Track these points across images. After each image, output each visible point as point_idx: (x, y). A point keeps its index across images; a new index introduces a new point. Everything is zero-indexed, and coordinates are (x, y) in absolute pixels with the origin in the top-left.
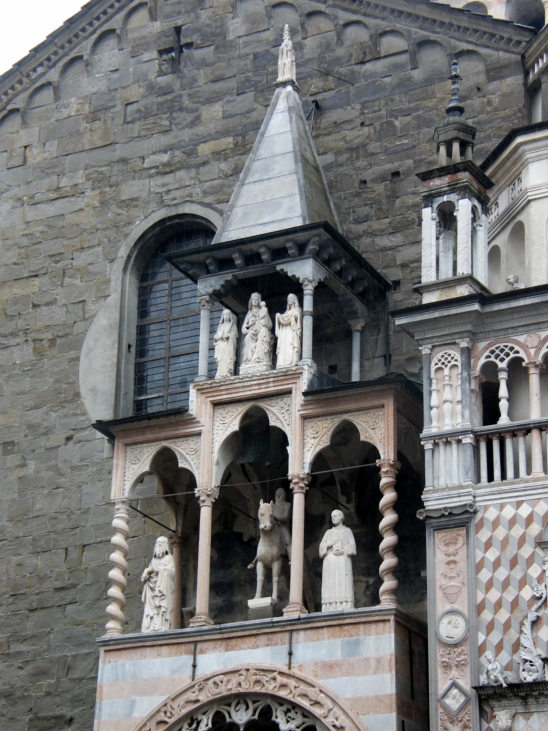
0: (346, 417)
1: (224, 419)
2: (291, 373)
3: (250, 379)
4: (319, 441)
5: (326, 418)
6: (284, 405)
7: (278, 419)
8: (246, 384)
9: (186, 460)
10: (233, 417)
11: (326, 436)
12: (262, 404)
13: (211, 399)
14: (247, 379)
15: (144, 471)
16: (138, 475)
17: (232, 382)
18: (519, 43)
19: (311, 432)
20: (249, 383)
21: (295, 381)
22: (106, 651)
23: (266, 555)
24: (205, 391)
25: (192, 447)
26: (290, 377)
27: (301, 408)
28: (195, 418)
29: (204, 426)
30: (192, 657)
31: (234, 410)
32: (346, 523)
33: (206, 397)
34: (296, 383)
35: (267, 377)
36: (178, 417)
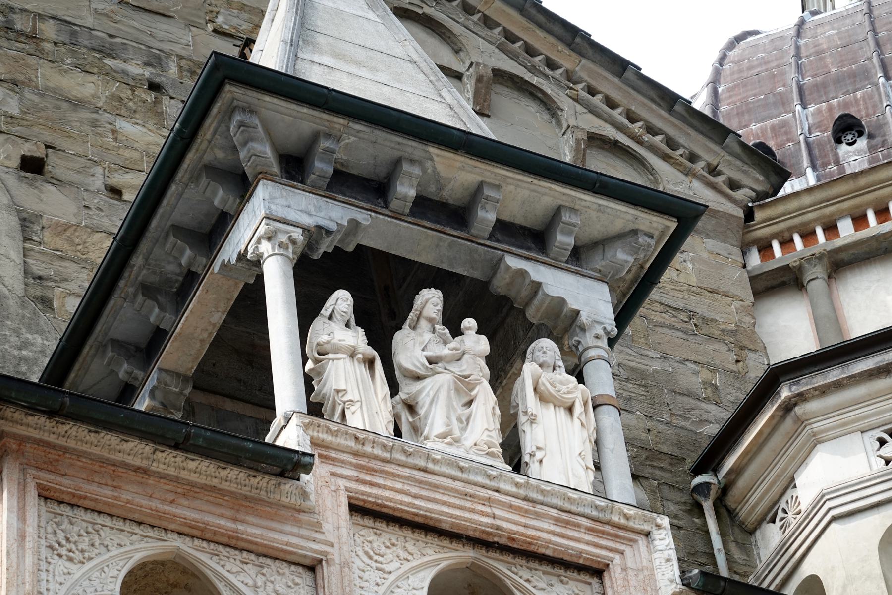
1: (380, 559)
2: (616, 518)
3: (487, 482)
10: (407, 566)
13: (353, 485)
14: (480, 479)
17: (430, 466)
18: (734, 185)
20: (483, 493)
24: (333, 454)
26: (607, 528)
28: (311, 511)
29: (332, 546)
31: (410, 546)
33: (333, 474)
34: (622, 553)
35: (540, 497)
36: (264, 482)
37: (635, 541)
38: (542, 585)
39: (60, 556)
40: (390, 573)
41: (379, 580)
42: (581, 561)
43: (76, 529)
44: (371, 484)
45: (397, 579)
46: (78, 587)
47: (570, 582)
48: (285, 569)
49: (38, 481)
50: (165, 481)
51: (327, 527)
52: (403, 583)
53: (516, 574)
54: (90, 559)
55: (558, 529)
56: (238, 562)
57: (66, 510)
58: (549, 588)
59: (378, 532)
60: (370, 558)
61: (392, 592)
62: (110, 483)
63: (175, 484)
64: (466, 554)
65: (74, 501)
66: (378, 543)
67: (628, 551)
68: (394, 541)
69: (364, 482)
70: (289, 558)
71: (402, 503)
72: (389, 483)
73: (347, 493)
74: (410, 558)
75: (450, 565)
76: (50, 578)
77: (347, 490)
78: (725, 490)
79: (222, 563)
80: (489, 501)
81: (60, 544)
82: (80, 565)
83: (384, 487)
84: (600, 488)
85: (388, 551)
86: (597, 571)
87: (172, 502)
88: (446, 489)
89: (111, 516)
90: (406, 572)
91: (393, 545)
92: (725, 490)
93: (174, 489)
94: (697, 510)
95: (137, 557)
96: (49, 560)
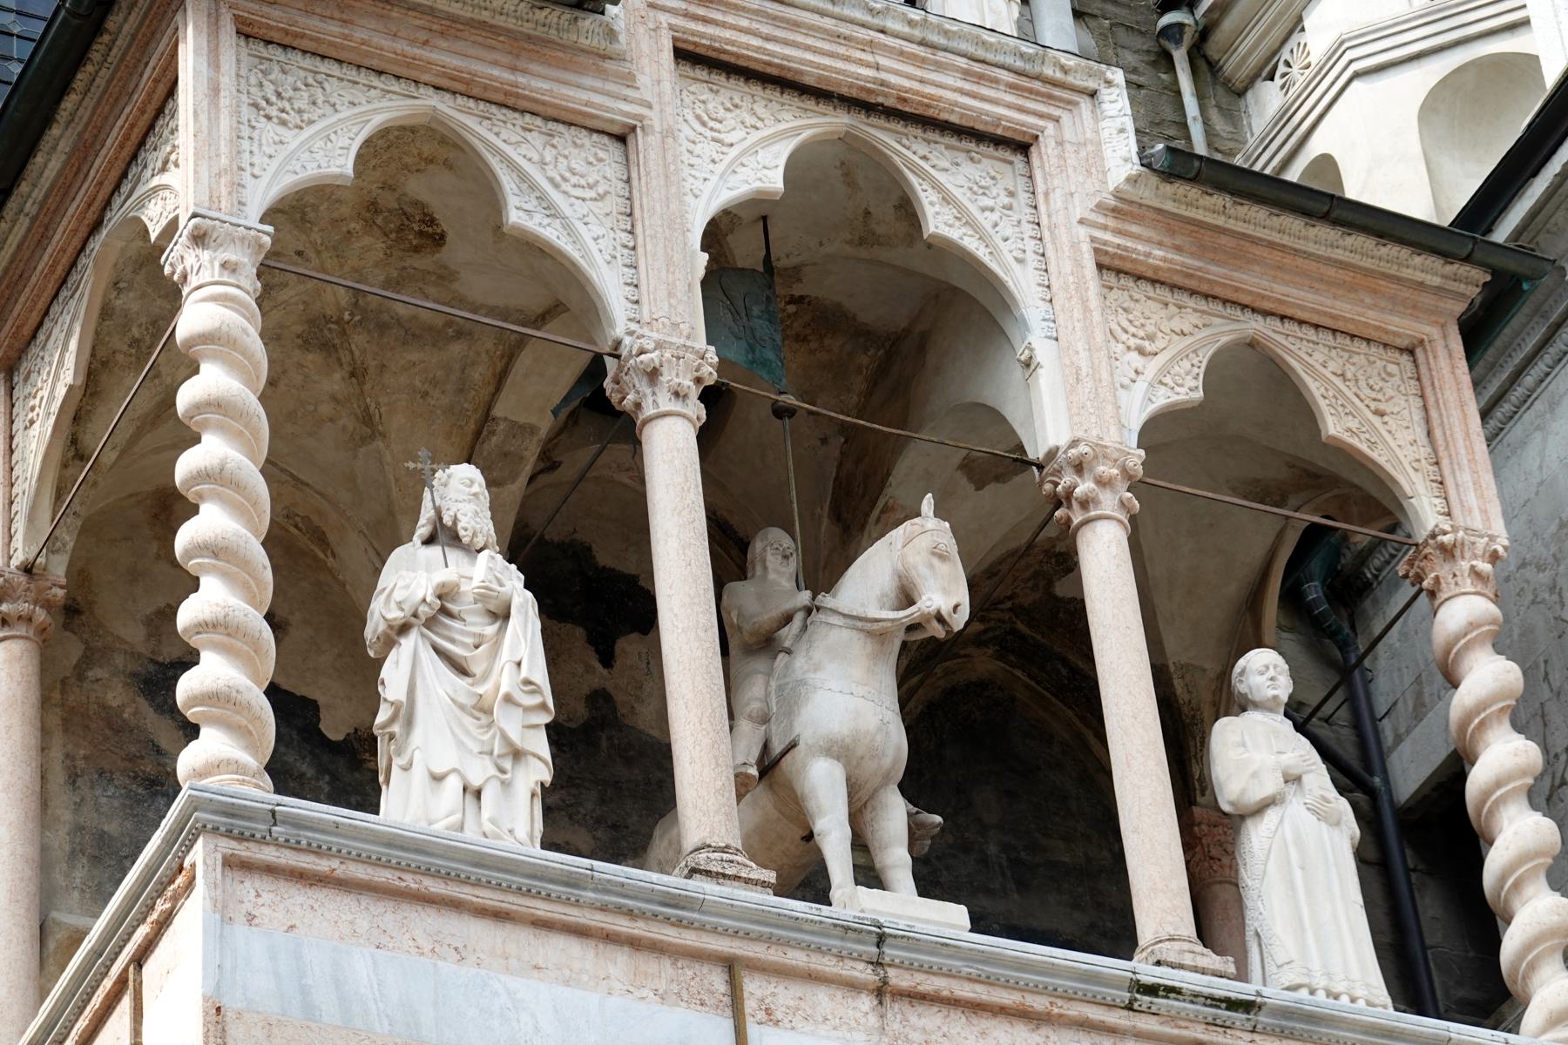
0: (1255, 326)
1: (717, 126)
2: (1049, 71)
3: (868, 18)
4: (1165, 370)
5: (1185, 299)
6: (989, 182)
7: (971, 223)
8: (845, 29)
9: (552, 212)
10: (755, 136)
11: (1186, 364)
12: (887, 138)
13: (680, 22)
15: (334, 170)
16: (302, 175)
19: (1125, 324)
21: (1056, 112)
22: (230, 863)
23: (879, 738)
25: (578, 168)
26: (1037, 85)
27: (1093, 217)
28: (620, 58)
29: (650, 107)
30: (726, 1025)
31: (759, 109)
32: (1300, 716)
35: (942, 41)
37: (1076, 104)
38: (946, 164)
39: (269, 118)
40: (732, 145)
41: (715, 156)
42: (999, 132)
43: (290, 79)
44: (705, 20)
45: (743, 153)
46: (294, 162)
47: (984, 160)
48: (585, 138)
49: (236, 12)
50: (414, 14)
51: (643, 80)
52: (750, 161)
53: (908, 149)
54: (311, 122)
55: (967, 86)
56: (518, 129)
57: (276, 53)
58: (954, 169)
59: (715, 87)
60: (704, 124)
61: (734, 172)
62: (337, 15)
63: (429, 18)
64: (838, 120)
65: (287, 41)
66: (715, 104)
67: (1066, 118)
68: (737, 100)
69: (695, 18)
70: (589, 123)
71: (748, 47)
72: (730, 19)
73: (672, 33)
74: (759, 124)
75: (814, 136)
76: (255, 149)
77: (671, 28)
78: (1204, 34)
79: (496, 129)
80: (871, 46)
81: (268, 101)
82: (297, 131)
83: (724, 25)
84: (1028, 29)
85: (729, 115)
86: (1022, 146)
87: (426, 43)
88: (811, 27)
89: (340, 62)
90: (754, 145)
91: (736, 106)
92: (1204, 34)
93: (427, 24)
94: (1165, 60)
95: (377, 121)
96: (254, 123)
